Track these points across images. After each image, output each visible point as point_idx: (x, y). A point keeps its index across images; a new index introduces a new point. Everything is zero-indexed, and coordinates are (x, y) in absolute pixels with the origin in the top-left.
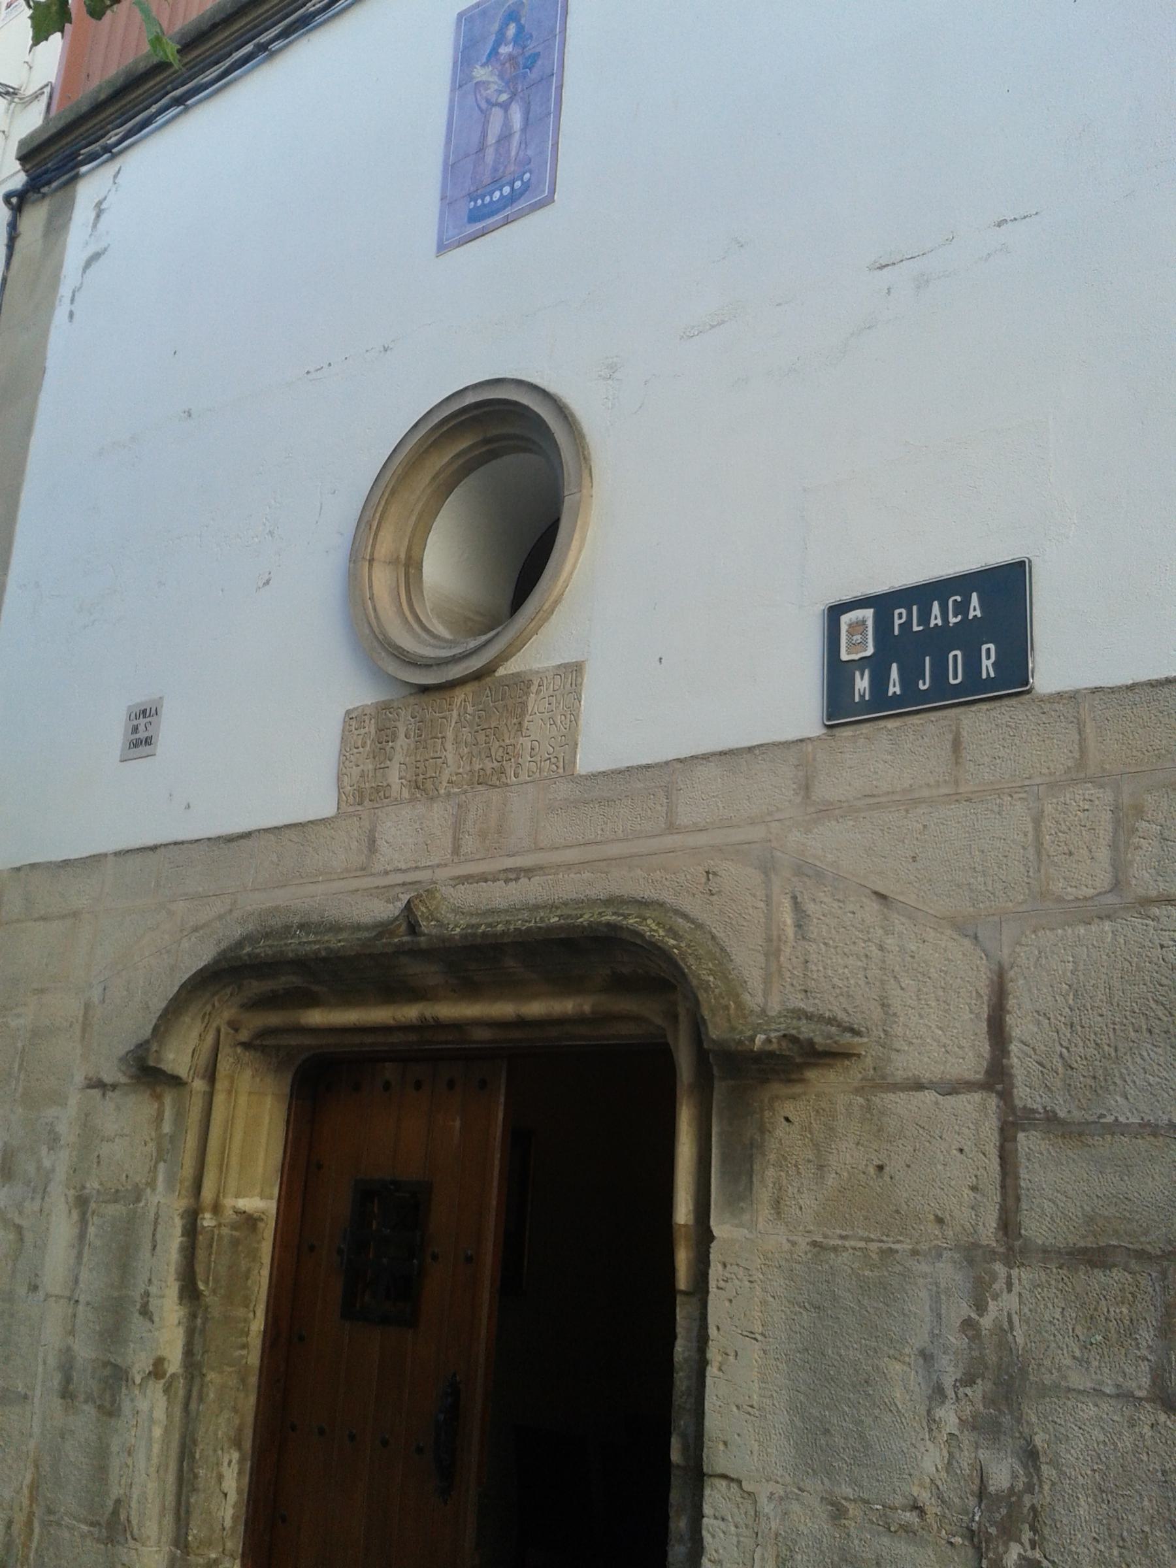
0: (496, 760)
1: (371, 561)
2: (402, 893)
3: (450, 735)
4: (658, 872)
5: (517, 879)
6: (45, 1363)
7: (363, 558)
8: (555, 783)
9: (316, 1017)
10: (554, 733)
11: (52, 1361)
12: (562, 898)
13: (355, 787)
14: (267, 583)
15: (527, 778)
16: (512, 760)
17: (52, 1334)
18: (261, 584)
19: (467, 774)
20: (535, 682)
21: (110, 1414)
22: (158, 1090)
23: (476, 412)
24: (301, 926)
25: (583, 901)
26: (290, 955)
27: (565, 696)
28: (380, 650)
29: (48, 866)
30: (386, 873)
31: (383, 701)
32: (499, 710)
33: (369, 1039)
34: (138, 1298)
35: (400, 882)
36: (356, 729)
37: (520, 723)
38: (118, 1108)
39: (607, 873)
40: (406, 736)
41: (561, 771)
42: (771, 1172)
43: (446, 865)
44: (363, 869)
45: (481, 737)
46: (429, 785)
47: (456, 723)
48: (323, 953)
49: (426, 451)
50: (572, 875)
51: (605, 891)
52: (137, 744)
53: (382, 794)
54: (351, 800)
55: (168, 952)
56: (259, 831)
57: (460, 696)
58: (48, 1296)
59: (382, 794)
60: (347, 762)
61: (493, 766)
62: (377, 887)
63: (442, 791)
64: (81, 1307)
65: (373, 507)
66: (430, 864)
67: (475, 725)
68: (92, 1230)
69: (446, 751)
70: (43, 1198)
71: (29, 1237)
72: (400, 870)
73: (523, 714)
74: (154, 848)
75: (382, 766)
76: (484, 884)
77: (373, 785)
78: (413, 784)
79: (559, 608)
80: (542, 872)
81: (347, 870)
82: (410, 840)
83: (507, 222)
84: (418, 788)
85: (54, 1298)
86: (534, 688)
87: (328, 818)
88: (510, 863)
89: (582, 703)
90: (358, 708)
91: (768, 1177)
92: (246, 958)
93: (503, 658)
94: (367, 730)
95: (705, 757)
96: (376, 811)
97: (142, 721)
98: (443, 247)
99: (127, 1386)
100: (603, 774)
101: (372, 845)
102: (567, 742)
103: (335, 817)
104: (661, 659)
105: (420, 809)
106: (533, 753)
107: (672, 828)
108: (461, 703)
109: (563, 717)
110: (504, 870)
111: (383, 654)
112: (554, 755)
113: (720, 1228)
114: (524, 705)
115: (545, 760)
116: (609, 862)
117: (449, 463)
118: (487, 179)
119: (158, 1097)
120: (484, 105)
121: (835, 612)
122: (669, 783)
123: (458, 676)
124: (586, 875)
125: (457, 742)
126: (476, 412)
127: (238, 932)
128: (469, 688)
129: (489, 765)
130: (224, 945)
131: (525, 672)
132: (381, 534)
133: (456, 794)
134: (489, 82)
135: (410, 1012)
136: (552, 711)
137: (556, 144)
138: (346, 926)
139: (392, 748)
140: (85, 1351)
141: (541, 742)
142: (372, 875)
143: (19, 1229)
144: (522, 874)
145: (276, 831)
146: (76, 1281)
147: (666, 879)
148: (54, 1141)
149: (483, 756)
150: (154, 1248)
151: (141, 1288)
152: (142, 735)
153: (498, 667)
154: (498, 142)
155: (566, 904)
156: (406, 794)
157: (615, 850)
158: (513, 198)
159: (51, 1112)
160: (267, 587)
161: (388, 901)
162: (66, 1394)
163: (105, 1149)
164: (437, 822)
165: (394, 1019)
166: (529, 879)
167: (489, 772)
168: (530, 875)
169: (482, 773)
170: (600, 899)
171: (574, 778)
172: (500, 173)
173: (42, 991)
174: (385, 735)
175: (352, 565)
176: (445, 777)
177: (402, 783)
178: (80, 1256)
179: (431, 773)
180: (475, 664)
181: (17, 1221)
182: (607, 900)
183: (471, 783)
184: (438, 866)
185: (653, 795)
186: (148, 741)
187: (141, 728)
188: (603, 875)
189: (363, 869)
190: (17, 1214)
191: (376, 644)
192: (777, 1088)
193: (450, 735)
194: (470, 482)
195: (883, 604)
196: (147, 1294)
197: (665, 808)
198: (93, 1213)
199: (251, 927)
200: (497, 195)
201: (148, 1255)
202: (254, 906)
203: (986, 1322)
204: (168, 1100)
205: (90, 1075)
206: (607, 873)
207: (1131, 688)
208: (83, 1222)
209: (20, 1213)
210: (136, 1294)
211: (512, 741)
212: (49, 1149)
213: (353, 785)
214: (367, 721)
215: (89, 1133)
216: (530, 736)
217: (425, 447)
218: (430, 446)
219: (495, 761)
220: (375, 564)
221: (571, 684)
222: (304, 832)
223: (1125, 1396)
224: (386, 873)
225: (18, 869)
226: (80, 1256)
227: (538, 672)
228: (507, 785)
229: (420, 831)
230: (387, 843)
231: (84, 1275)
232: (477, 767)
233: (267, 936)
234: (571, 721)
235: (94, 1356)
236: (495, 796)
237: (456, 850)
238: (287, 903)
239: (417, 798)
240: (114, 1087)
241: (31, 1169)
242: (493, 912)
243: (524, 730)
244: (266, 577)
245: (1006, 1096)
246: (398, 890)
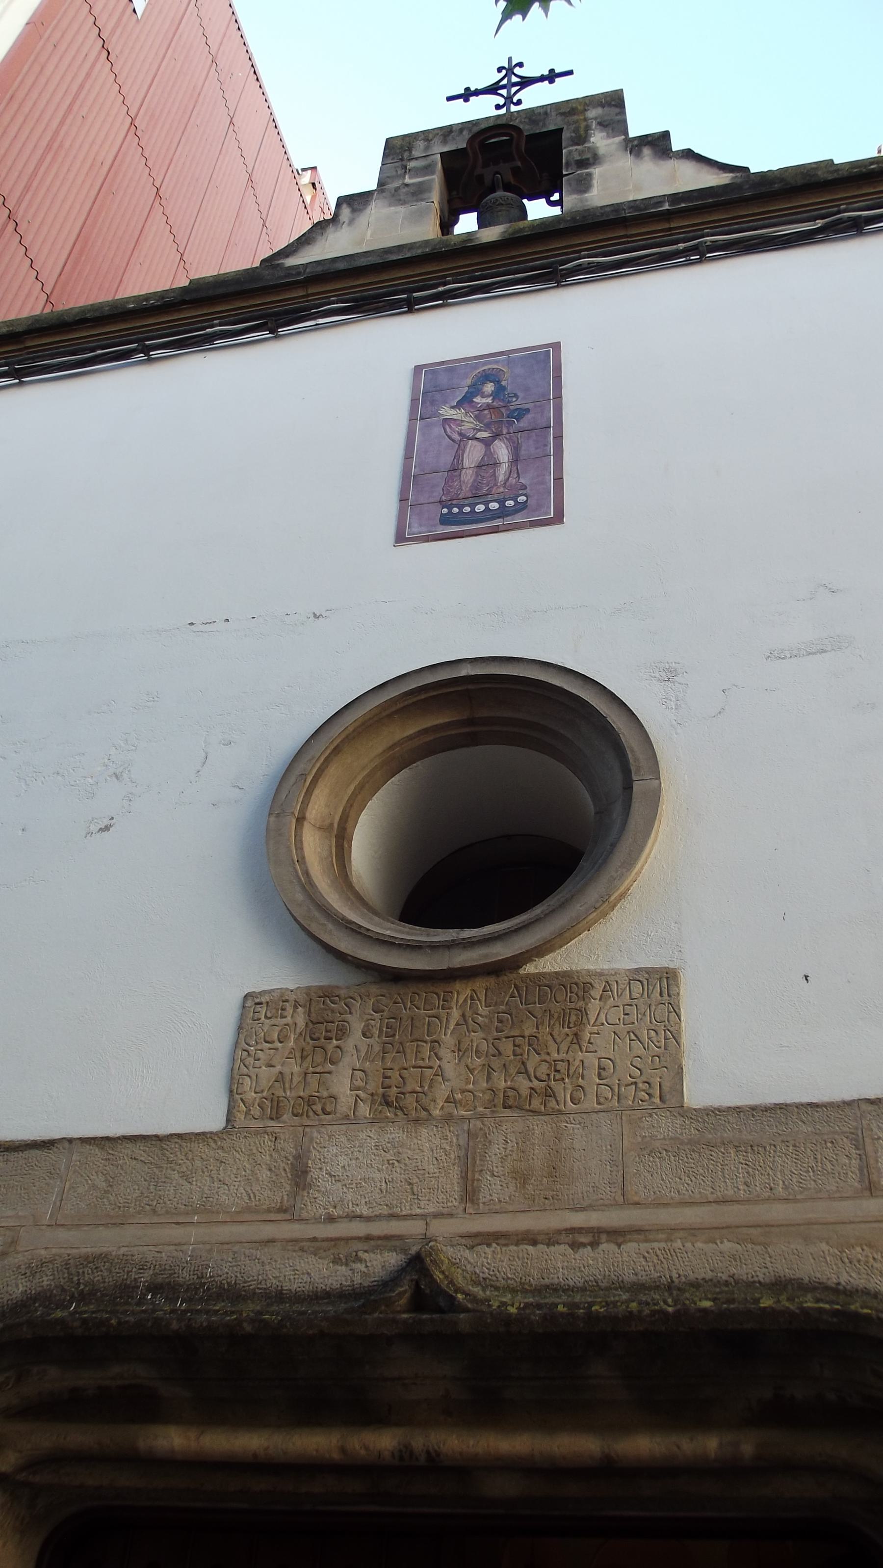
0: (536, 1077)
1: (301, 820)
2: (366, 1251)
3: (448, 1040)
4: (859, 1249)
5: (594, 1244)
7: (293, 813)
8: (651, 1115)
10: (641, 1051)
12: (686, 1276)
13: (265, 1094)
14: (107, 828)
15: (596, 1105)
16: (567, 1080)
18: (94, 828)
19: (484, 1093)
20: (596, 985)
23: (470, 687)
24: (155, 1288)
25: (727, 1283)
26: (175, 1325)
27: (653, 1008)
28: (323, 920)
30: (331, 1219)
31: (320, 988)
32: (536, 1014)
35: (361, 1234)
36: (266, 1017)
37: (576, 1035)
39: (765, 1245)
40: (364, 1035)
41: (657, 1101)
43: (451, 1215)
44: (282, 1210)
45: (507, 1047)
46: (410, 1101)
47: (458, 1024)
48: (248, 1328)
49: (389, 716)
50: (699, 1245)
51: (764, 1270)
53: (318, 1108)
54: (256, 1111)
56: (70, 1141)
57: (462, 992)
59: (318, 1108)
60: (250, 1061)
61: (531, 1085)
62: (314, 1239)
63: (436, 1112)
65: (310, 760)
66: (419, 1211)
67: (493, 1029)
69: (439, 1059)
72: (360, 1217)
73: (580, 1023)
75: (318, 1070)
76: (530, 1248)
77: (302, 1094)
78: (379, 1099)
79: (624, 903)
80: (642, 1237)
81: (248, 1210)
82: (377, 1176)
83: (495, 530)
84: (388, 1104)
86: (596, 993)
87: (211, 1133)
88: (577, 1220)
89: (682, 1019)
90: (273, 990)
92: (77, 1324)
93: (540, 951)
94: (289, 1020)
96: (307, 1130)
98: (401, 538)
100: (738, 1110)
102: (665, 1064)
103: (224, 1131)
104: (806, 977)
105: (395, 1133)
106: (603, 1073)
108: (465, 1000)
109: (653, 1033)
110: (566, 1230)
111: (330, 926)
112: (644, 1078)
114: (583, 1013)
115: (627, 1085)
116: (767, 1229)
117: (410, 738)
118: (465, 491)
120: (456, 437)
122: (857, 1128)
123: (467, 965)
124: (727, 1246)
125: (459, 1049)
126: (470, 687)
127: (18, 1288)
128: (480, 984)
129: (523, 1084)
131: (577, 972)
132: (316, 792)
133: (463, 1118)
134: (462, 421)
136: (633, 1023)
137: (559, 480)
138: (255, 1293)
139: (338, 1047)
141: (618, 1061)
142: (301, 1220)
144: (604, 1237)
145: (108, 1144)
147: (874, 1259)
149: (513, 1071)
153: (526, 964)
154: (479, 466)
155: (695, 1285)
156: (364, 1109)
157: (778, 1212)
158: (503, 512)
160: (106, 834)
161: (336, 1261)
164: (427, 1153)
165: (343, 1450)
166: (619, 1246)
167: (525, 1092)
168: (620, 1240)
169: (511, 1093)
170: (760, 1282)
171: (682, 1110)
172: (485, 490)
175: (272, 819)
176: (442, 1091)
177: (357, 1096)
180: (501, 951)
182: (773, 1285)
183: (491, 1105)
184: (437, 1216)
185: (832, 1142)
188: (758, 1248)
189: (282, 1210)
191: (317, 914)
193: (448, 1040)
194: (420, 766)
197: (855, 1163)
199: (46, 1281)
200: (480, 508)
202: (54, 1251)
206: (765, 1245)
211: (563, 1055)
213: (262, 1091)
214: (290, 1010)
216: (596, 1051)
217: (388, 712)
218: (397, 712)
219: (534, 1079)
220: (306, 825)
221: (661, 995)
222: (162, 1149)
224: (331, 1219)
227: (601, 974)
228: (560, 1112)
229: (396, 1164)
230: (331, 1176)
232: (503, 1084)
233: (83, 1298)
234: (666, 1039)
236: (539, 1126)
238: (123, 1250)
239: (387, 1117)
242: (555, 1289)
243: (585, 1045)
244: (106, 822)
246: (358, 1246)
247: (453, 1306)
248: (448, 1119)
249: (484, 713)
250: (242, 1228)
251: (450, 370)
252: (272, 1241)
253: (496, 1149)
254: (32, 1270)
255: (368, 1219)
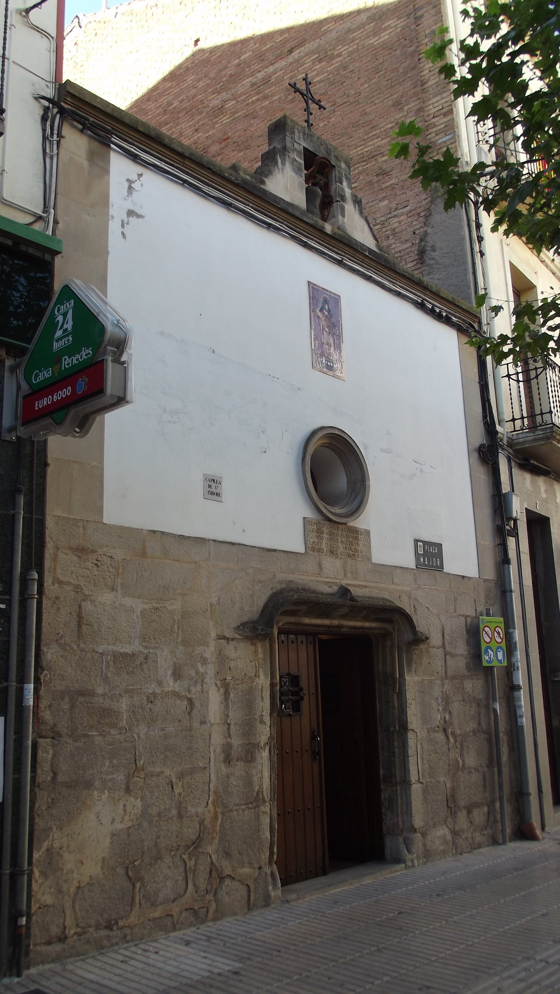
6: (215, 751)
9: (307, 621)
11: (218, 750)
14: (265, 452)
17: (217, 739)
21: (250, 762)
22: (254, 641)
24: (303, 589)
29: (174, 535)
33: (312, 628)
34: (258, 718)
38: (235, 648)
42: (414, 665)
46: (335, 552)
52: (212, 493)
55: (248, 588)
58: (212, 725)
64: (232, 727)
68: (232, 695)
70: (202, 686)
71: (197, 704)
74: (233, 544)
85: (216, 725)
91: (414, 666)
95: (398, 567)
97: (213, 485)
99: (258, 750)
101: (320, 565)
107: (393, 583)
113: (407, 678)
119: (255, 645)
121: (416, 541)
127: (279, 587)
129: (351, 553)
130: (274, 590)
135: (327, 622)
140: (236, 742)
143: (190, 700)
146: (228, 716)
148: (204, 661)
150: (262, 699)
151: (259, 714)
152: (213, 490)
159: (199, 649)
162: (228, 760)
163: (232, 664)
173: (184, 594)
174: (319, 532)
178: (227, 707)
179: (335, 549)
181: (188, 696)
186: (218, 495)
187: (213, 487)
189: (319, 574)
190: (187, 693)
192: (414, 647)
195: (425, 543)
196: (262, 716)
198: (232, 689)
199: (284, 586)
201: (260, 702)
203: (444, 690)
204: (259, 645)
205: (219, 634)
207: (455, 575)
208: (226, 694)
209: (189, 692)
210: (257, 717)
212: (202, 664)
215: (222, 658)
223: (460, 701)
225: (154, 532)
226: (227, 707)
231: (230, 714)
235: (242, 742)
237: (345, 575)
240: (233, 639)
241: (193, 673)
245: (445, 649)
247: (357, 601)
248: (341, 558)
249: (333, 443)
250: (313, 578)
251: (317, 290)
252: (318, 581)
253: (348, 566)
254: (281, 582)
255: (332, 578)
